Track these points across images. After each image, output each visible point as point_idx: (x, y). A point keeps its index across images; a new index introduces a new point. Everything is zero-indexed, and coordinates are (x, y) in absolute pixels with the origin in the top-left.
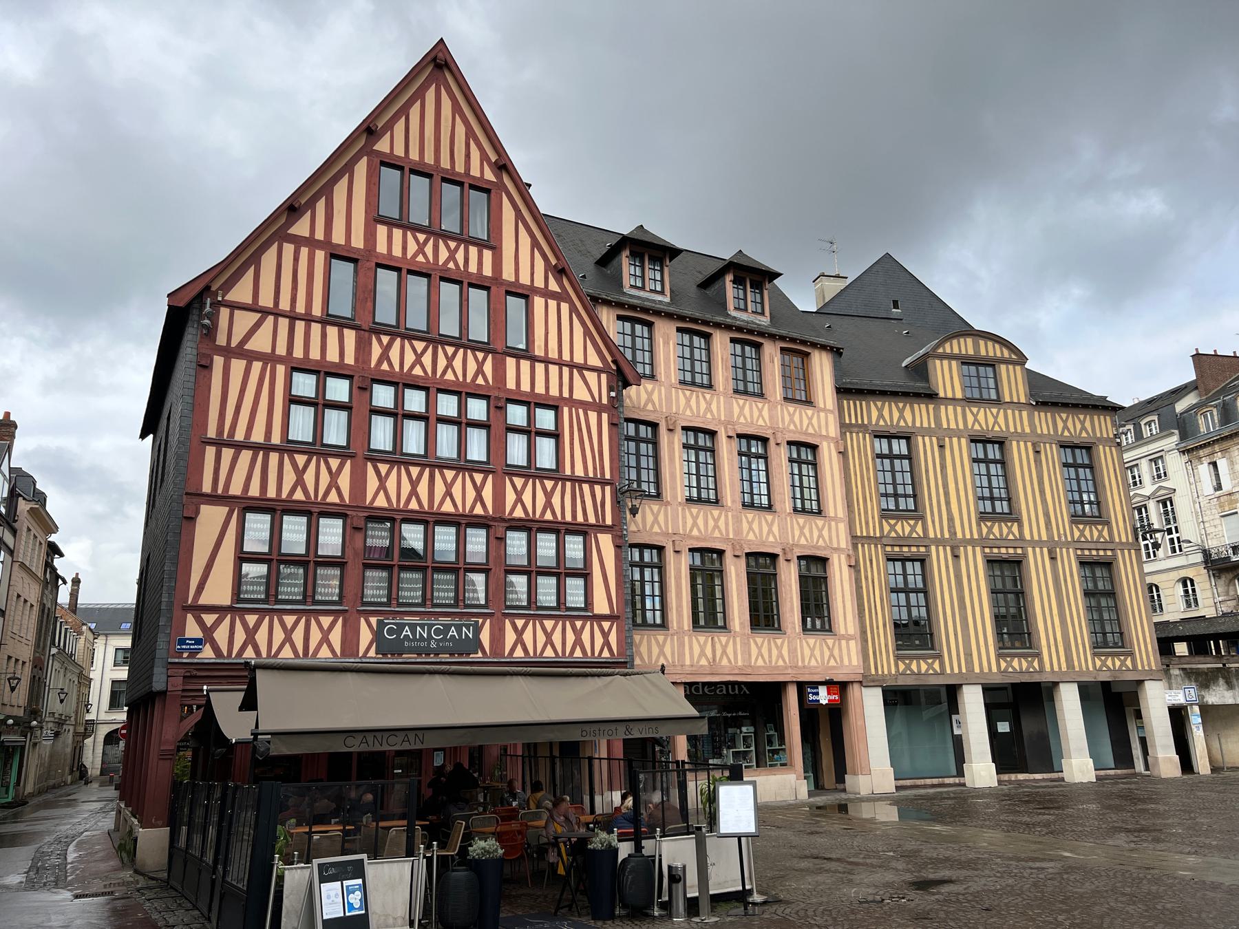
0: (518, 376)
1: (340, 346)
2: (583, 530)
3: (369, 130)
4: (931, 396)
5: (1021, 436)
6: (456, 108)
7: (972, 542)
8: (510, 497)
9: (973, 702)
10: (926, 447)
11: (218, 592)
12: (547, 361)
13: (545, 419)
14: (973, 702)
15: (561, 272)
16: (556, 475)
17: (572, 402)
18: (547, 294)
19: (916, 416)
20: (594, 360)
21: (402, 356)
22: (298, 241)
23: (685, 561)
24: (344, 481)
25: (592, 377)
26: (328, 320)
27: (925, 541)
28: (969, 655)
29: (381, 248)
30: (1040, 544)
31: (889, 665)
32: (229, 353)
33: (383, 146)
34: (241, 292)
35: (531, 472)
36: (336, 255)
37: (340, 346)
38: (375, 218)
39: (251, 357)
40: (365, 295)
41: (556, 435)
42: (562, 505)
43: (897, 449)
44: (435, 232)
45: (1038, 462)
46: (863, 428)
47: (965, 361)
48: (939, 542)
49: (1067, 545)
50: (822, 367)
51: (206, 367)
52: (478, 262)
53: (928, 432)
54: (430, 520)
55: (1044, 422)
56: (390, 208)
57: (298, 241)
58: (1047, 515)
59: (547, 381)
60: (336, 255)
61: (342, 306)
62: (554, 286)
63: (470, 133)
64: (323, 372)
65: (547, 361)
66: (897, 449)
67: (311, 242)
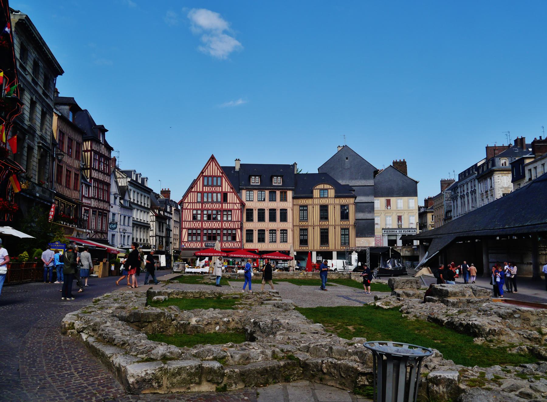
0: (225, 206)
1: (199, 206)
2: (235, 229)
3: (202, 172)
4: (312, 197)
5: (331, 204)
6: (216, 165)
7: (318, 226)
8: (224, 225)
9: (314, 254)
10: (310, 208)
11: (186, 240)
12: (230, 203)
13: (230, 213)
14: (314, 254)
15: (232, 188)
16: (231, 221)
17: (234, 209)
18: (230, 192)
19: (308, 202)
20: (238, 202)
21: (208, 206)
22: (193, 192)
23: (257, 231)
24: (200, 225)
25: (237, 205)
26: (197, 202)
27: (308, 226)
28: (314, 246)
29: (204, 190)
30: (332, 225)
31: (298, 247)
32: (185, 209)
33: (204, 174)
34: (186, 201)
35: (227, 221)
36: (198, 192)
37: (199, 206)
38: (203, 186)
39: (188, 209)
40: (202, 198)
41: (231, 215)
42: (232, 226)
43: (304, 208)
44: (212, 186)
45: (335, 209)
46: (297, 205)
47: (321, 190)
48: (310, 226)
49: (338, 225)
50: (290, 194)
51: (182, 212)
52: (219, 189)
53: (311, 205)
54: (212, 229)
55: (337, 201)
56: (206, 184)
57: (193, 192)
58: (335, 220)
59: (230, 207)
60: (198, 192)
61: (199, 200)
62: (231, 191)
63: (218, 168)
64: (197, 210)
65: (230, 203)
66: (304, 208)
67: (195, 192)
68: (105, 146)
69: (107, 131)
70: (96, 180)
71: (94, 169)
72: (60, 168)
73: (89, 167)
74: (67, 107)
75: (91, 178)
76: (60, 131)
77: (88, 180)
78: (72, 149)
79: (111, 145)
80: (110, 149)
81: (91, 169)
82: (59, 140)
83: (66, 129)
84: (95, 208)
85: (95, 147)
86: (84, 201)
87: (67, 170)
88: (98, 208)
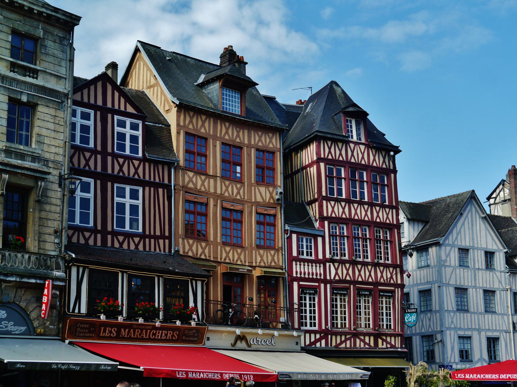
68: (368, 146)
69: (368, 114)
70: (335, 221)
71: (328, 199)
72: (197, 208)
73: (316, 197)
74: (216, 87)
75: (322, 219)
76: (187, 134)
77: (317, 225)
78: (240, 165)
79: (391, 138)
80: (390, 150)
81: (321, 199)
82: (187, 151)
83: (205, 127)
84: (340, 281)
85: (336, 152)
86: (297, 269)
87: (224, 209)
88: (354, 282)
